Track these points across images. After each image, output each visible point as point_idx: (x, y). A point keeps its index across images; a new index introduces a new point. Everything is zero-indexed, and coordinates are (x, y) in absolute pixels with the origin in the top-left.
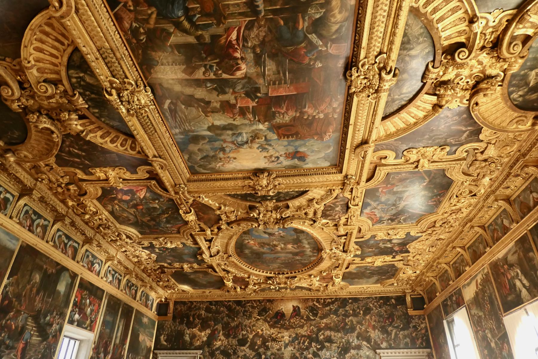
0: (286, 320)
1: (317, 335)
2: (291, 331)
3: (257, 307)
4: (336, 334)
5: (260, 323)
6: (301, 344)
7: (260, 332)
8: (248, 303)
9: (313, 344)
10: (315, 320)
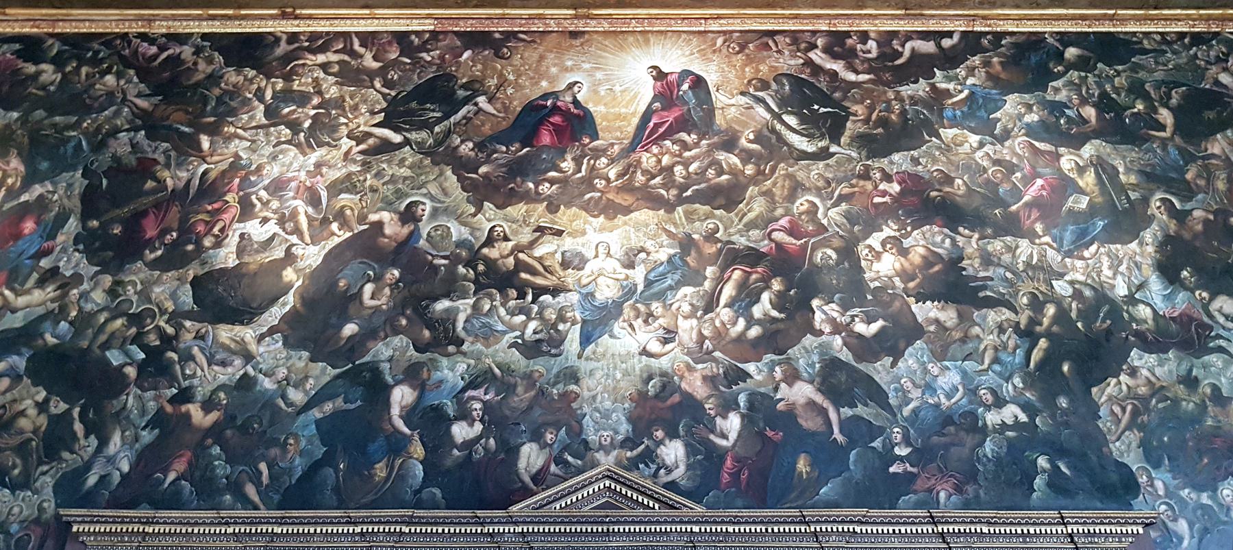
0: (598, 153)
1: (848, 252)
3: (382, 72)
4: (996, 246)
6: (724, 314)
7: (393, 228)
8: (323, 49)
9: (823, 311)
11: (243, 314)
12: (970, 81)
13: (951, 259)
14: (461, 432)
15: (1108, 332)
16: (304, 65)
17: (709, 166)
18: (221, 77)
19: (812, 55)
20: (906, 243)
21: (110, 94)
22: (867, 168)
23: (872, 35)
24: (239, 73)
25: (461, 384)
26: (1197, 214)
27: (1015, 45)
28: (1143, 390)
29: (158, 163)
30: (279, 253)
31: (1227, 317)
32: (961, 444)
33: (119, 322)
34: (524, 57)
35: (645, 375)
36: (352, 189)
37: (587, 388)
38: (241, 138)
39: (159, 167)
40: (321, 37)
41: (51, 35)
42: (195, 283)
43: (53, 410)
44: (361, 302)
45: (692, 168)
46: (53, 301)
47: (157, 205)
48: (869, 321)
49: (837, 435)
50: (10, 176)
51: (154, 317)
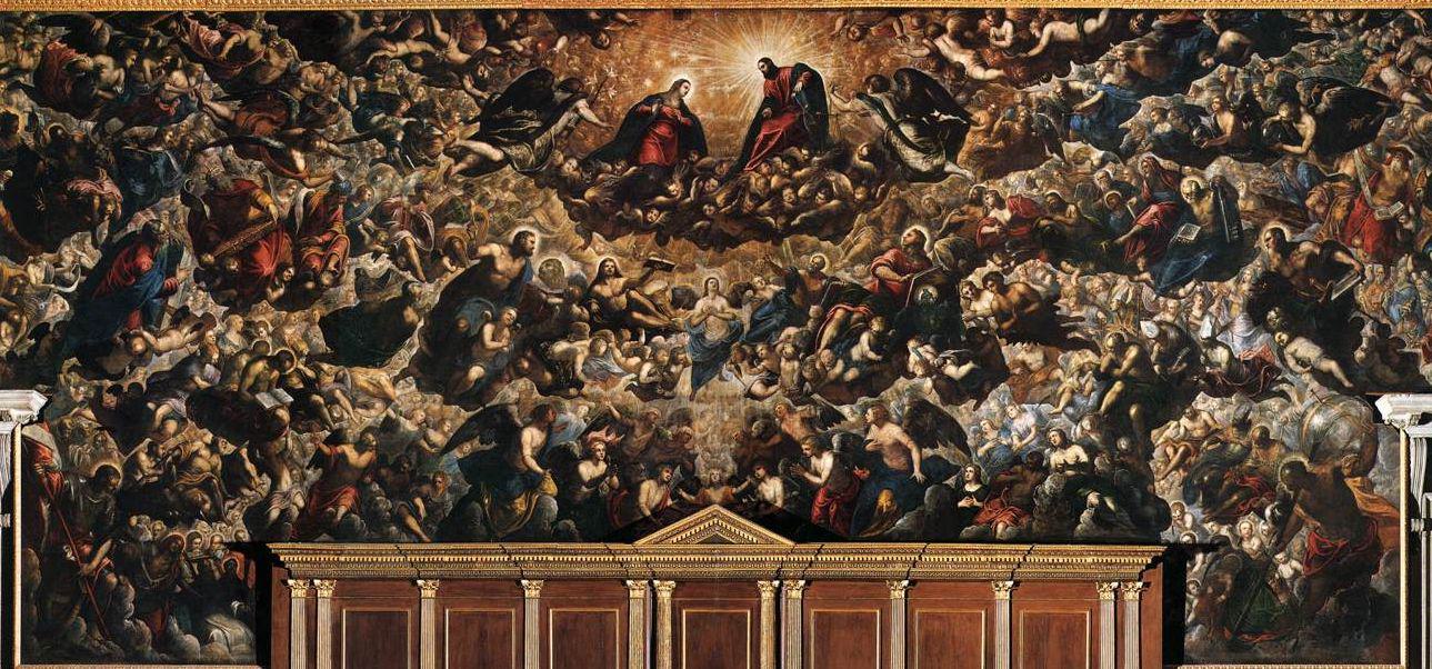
0: (707, 173)
1: (949, 292)
2: (745, 259)
3: (470, 67)
4: (1095, 283)
5: (502, 191)
7: (505, 264)
8: (401, 36)
10: (938, 174)
11: (375, 356)
12: (1105, 80)
13: (1049, 297)
14: (587, 470)
15: (1182, 375)
16: (384, 57)
17: (819, 189)
18: (299, 74)
19: (939, 43)
20: (1008, 279)
21: (183, 96)
22: (981, 191)
23: (1010, 14)
24: (317, 69)
25: (584, 426)
26: (1305, 247)
27: (1167, 28)
28: (1198, 433)
29: (257, 187)
30: (397, 292)
31: (1302, 362)
32: (1025, 481)
33: (260, 366)
34: (626, 45)
35: (750, 417)
36: (458, 218)
37: (699, 428)
38: (336, 155)
39: (258, 192)
40: (398, 19)
41: (99, 15)
42: (323, 323)
43: (226, 452)
44: (483, 344)
45: (800, 192)
46: (193, 342)
47: (266, 236)
48: (959, 364)
49: (917, 474)
50: (108, 202)
51: (292, 360)
